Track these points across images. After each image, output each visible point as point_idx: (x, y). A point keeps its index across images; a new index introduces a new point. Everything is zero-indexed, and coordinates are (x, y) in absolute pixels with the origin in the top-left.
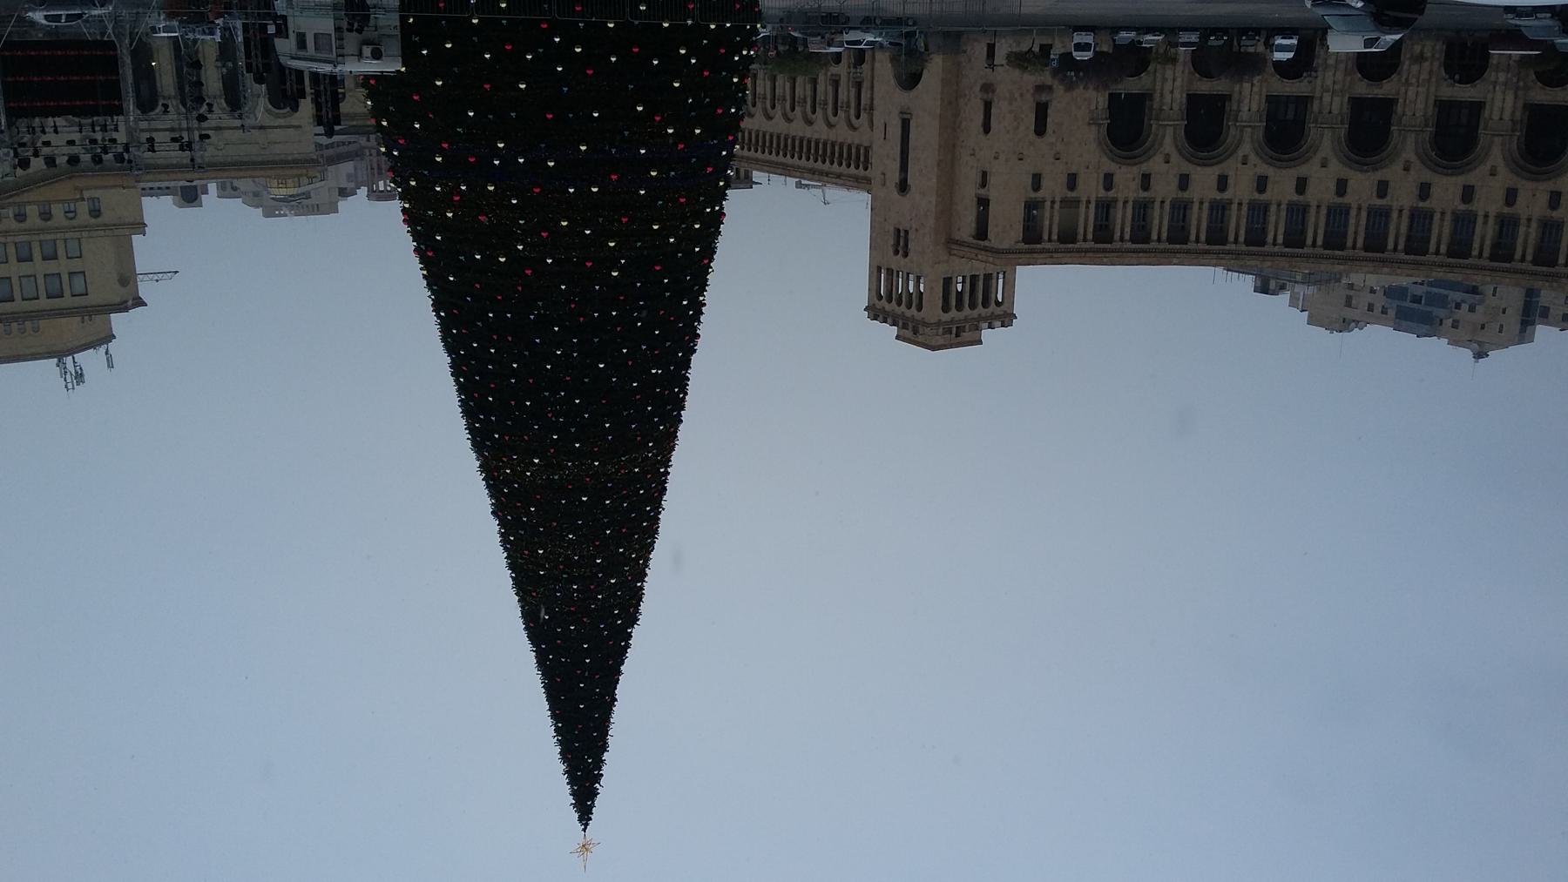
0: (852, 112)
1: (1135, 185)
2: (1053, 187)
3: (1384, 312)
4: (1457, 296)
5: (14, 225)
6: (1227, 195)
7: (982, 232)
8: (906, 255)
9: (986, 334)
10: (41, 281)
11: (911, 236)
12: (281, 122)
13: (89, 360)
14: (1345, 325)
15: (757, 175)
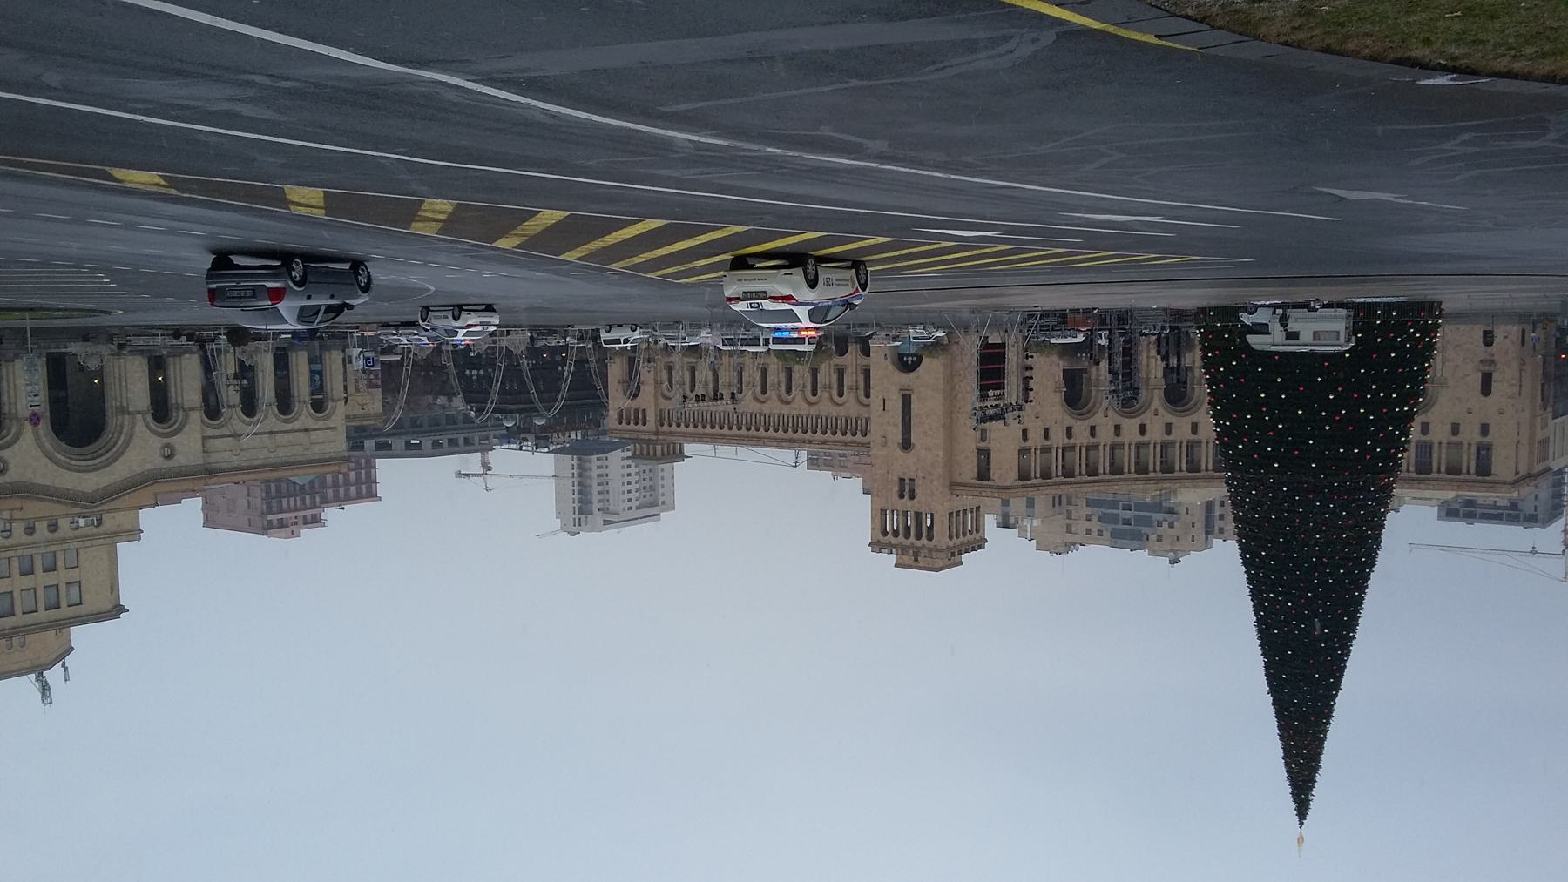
0: (835, 392)
1: (1088, 432)
2: (1036, 439)
3: (1100, 533)
4: (1157, 516)
5: (25, 539)
6: (1145, 438)
7: (984, 474)
8: (912, 497)
9: (965, 557)
10: (40, 592)
11: (918, 482)
12: (321, 424)
13: (54, 675)
14: (1069, 547)
15: (689, 448)
